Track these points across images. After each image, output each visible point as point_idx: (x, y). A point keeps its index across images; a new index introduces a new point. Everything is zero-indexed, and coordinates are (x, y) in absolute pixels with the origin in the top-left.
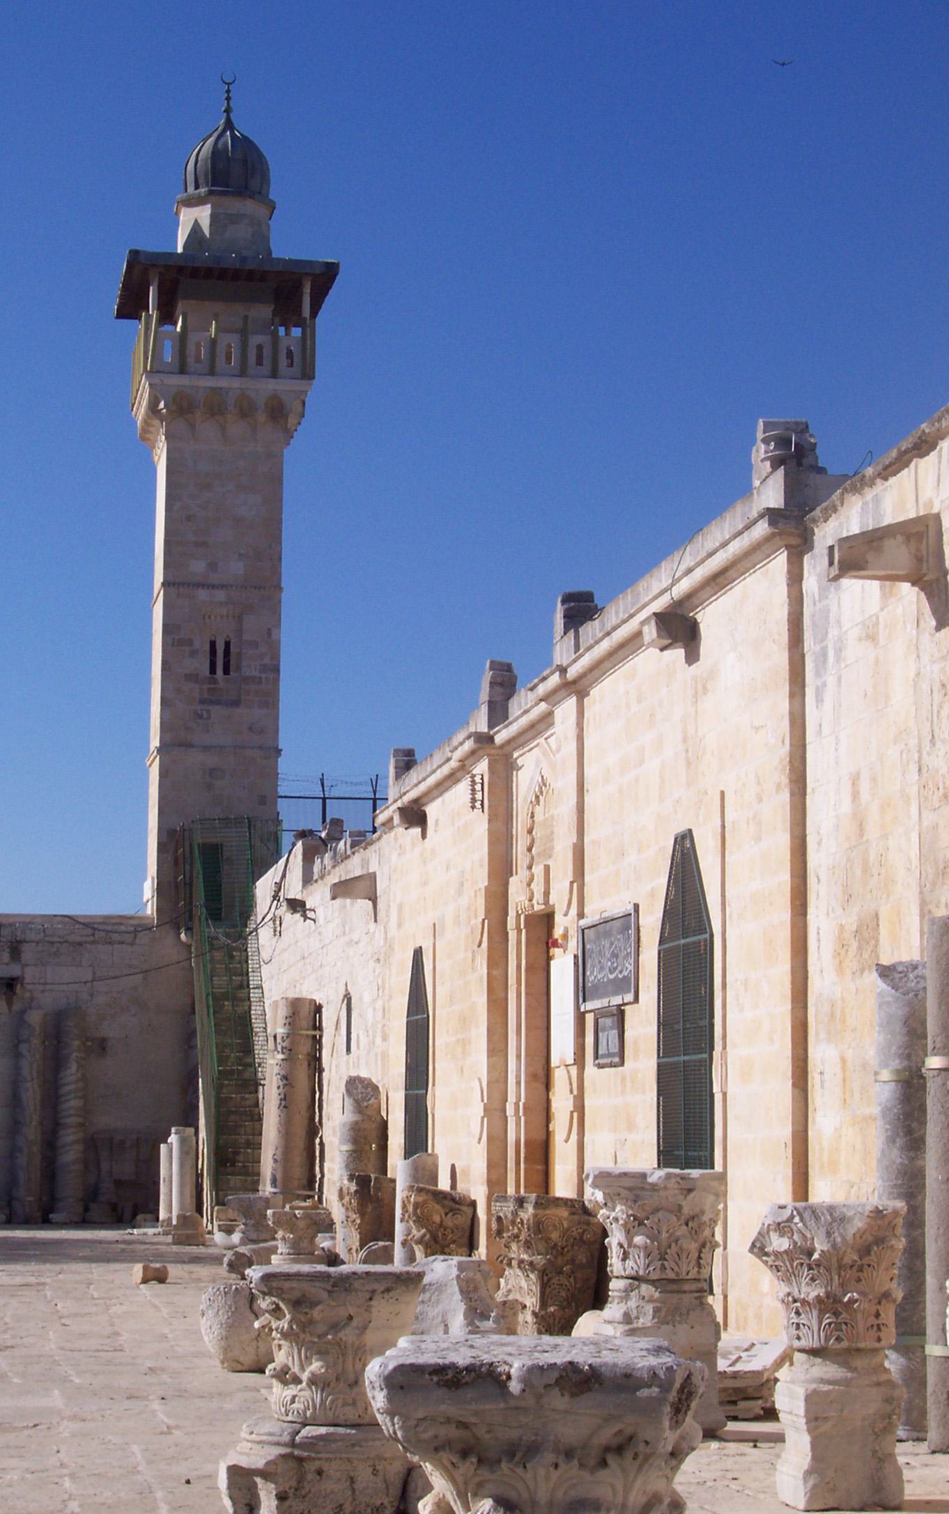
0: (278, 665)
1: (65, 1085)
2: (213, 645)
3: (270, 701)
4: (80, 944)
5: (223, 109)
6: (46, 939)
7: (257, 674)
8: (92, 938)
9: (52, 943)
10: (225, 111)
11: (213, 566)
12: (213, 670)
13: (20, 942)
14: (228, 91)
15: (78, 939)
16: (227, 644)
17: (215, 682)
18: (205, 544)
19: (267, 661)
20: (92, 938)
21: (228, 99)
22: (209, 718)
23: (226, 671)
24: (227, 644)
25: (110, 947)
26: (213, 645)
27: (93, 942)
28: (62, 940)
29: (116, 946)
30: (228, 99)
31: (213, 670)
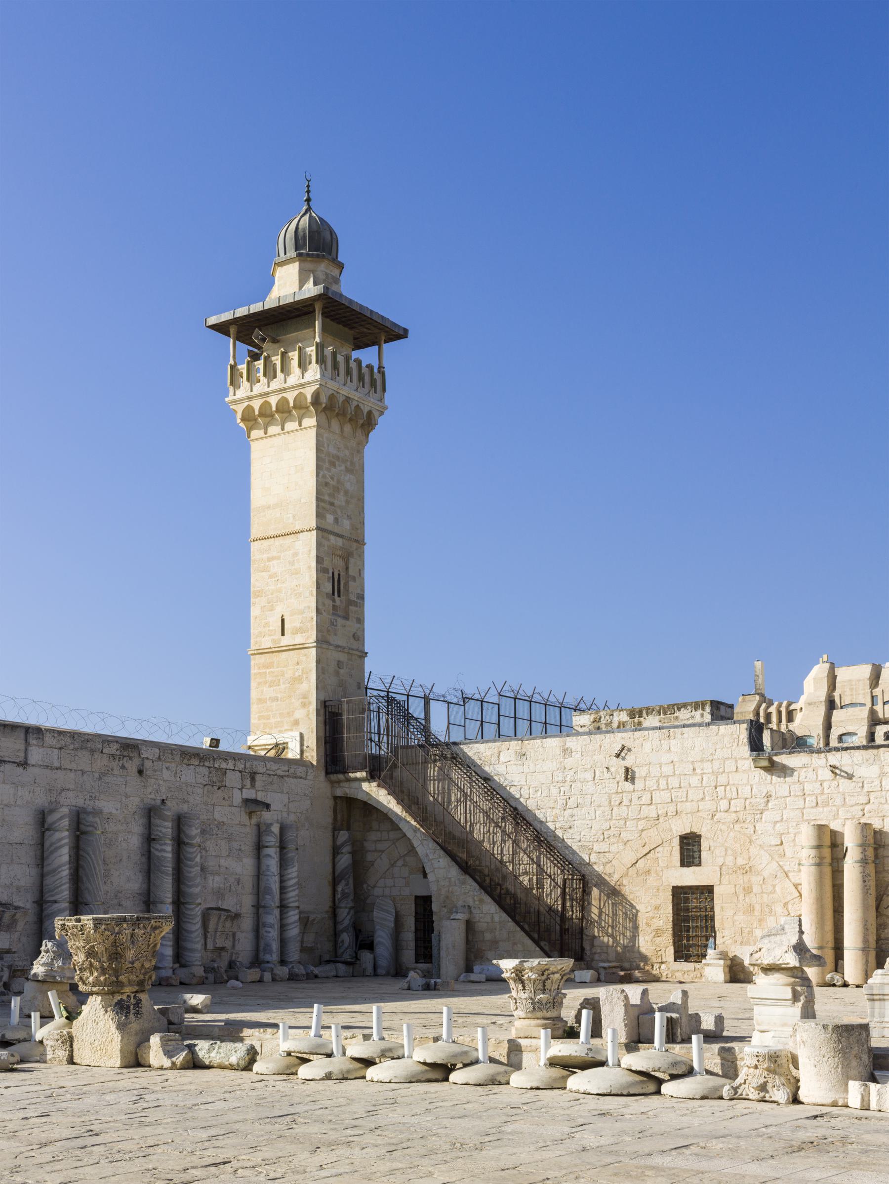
0: (363, 595)
1: (289, 879)
2: (333, 574)
3: (360, 621)
4: (282, 777)
5: (305, 198)
6: (268, 772)
7: (355, 599)
8: (287, 773)
9: (269, 775)
10: (306, 201)
11: (336, 520)
12: (333, 594)
13: (255, 773)
14: (308, 186)
15: (282, 773)
16: (339, 575)
17: (334, 601)
18: (332, 504)
19: (359, 591)
20: (287, 773)
21: (308, 192)
22: (336, 626)
23: (339, 596)
24: (339, 575)
25: (295, 780)
26: (333, 574)
27: (288, 776)
28: (274, 773)
29: (299, 780)
30: (308, 192)
31: (333, 594)
